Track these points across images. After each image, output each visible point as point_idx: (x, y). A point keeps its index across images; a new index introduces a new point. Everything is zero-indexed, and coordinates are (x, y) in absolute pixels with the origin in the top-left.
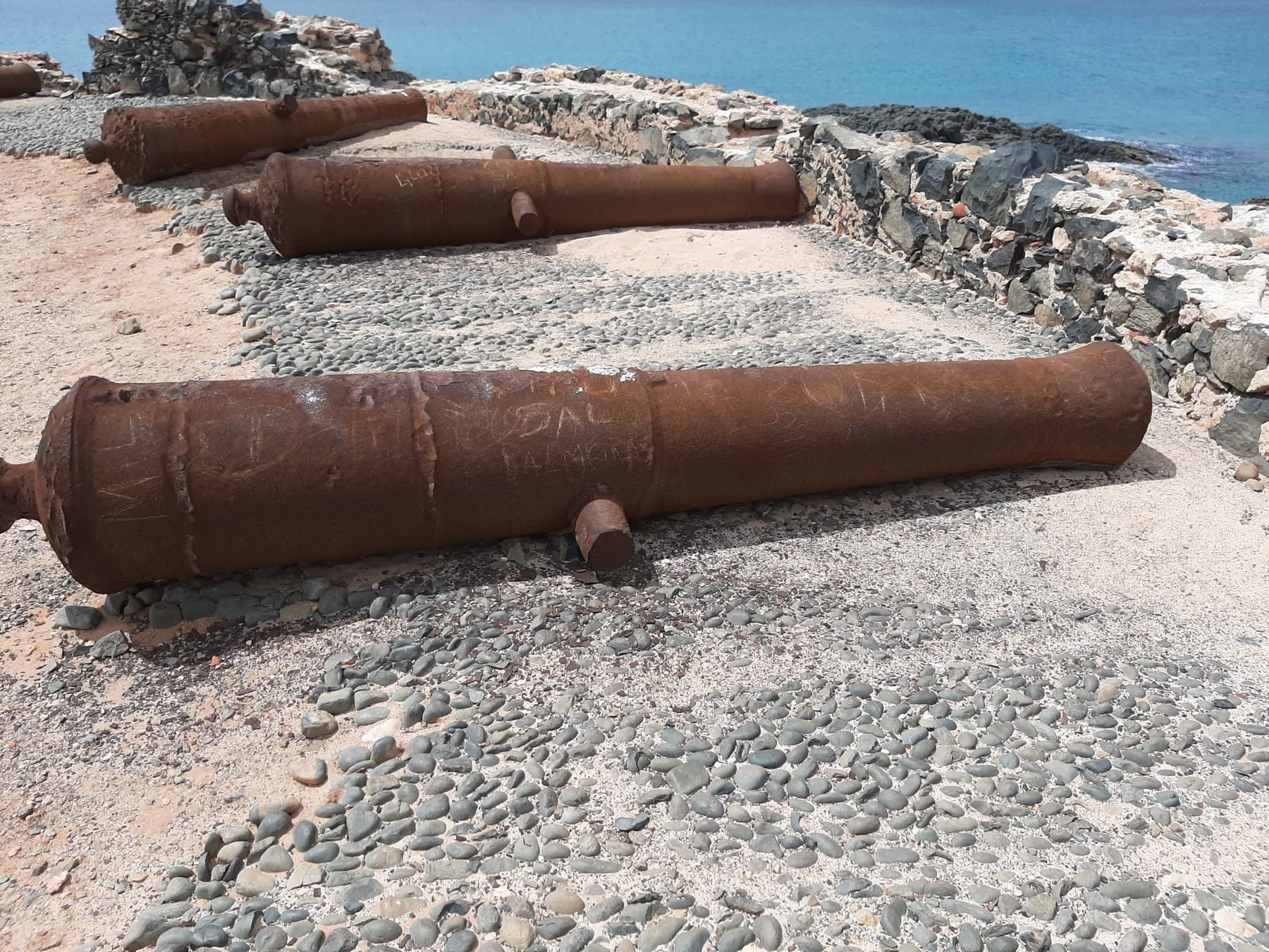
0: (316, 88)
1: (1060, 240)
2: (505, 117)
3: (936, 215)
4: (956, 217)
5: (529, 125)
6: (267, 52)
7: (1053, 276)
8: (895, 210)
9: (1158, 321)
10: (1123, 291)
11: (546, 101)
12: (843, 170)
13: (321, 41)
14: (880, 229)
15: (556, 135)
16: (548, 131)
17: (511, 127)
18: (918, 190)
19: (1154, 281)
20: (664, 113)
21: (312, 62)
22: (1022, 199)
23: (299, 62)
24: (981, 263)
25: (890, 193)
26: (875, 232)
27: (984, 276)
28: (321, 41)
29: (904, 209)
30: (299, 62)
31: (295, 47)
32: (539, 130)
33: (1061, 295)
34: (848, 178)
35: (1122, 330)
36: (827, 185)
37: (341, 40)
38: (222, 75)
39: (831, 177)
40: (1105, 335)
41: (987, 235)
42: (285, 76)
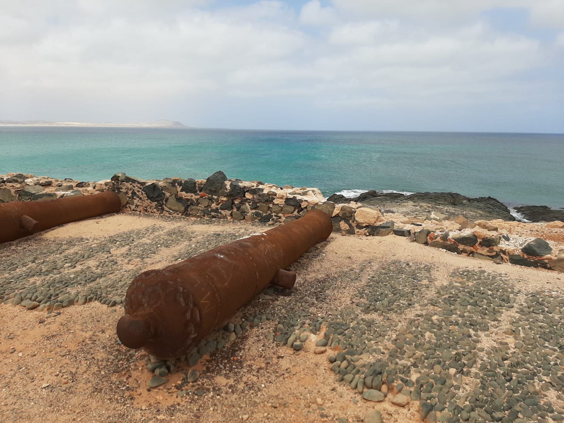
1: (248, 196)
3: (193, 198)
4: (201, 197)
7: (249, 207)
8: (172, 200)
9: (293, 209)
10: (277, 204)
12: (140, 190)
14: (165, 207)
18: (182, 191)
19: (287, 200)
20: (10, 182)
22: (228, 187)
24: (217, 209)
25: (168, 194)
26: (163, 209)
27: (220, 213)
29: (176, 198)
33: (254, 211)
34: (144, 192)
35: (280, 215)
36: (132, 196)
39: (134, 193)
40: (274, 217)
41: (217, 200)
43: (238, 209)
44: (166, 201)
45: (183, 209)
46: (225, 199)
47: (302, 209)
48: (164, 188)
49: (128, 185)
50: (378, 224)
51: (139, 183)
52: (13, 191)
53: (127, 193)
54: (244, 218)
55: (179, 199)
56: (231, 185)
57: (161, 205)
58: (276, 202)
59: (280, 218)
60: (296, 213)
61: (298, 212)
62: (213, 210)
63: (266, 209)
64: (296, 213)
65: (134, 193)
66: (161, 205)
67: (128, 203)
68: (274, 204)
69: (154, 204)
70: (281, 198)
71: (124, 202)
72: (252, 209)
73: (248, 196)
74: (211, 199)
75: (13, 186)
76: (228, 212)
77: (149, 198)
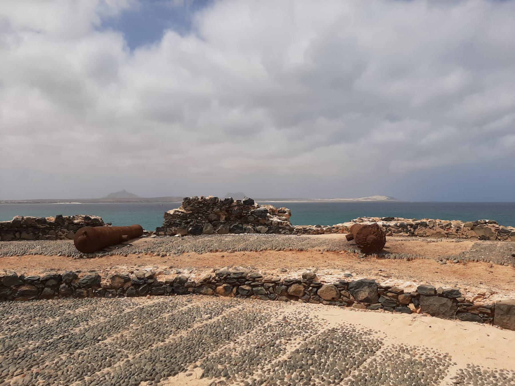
0: (280, 228)
5: (401, 234)
6: (256, 217)
11: (411, 226)
13: (273, 212)
15: (416, 236)
16: (413, 235)
20: (491, 223)
21: (275, 219)
23: (271, 219)
28: (273, 212)
30: (271, 219)
31: (268, 214)
32: (407, 235)
37: (279, 212)
38: (230, 226)
42: (264, 224)
52: (493, 229)
75: (493, 226)
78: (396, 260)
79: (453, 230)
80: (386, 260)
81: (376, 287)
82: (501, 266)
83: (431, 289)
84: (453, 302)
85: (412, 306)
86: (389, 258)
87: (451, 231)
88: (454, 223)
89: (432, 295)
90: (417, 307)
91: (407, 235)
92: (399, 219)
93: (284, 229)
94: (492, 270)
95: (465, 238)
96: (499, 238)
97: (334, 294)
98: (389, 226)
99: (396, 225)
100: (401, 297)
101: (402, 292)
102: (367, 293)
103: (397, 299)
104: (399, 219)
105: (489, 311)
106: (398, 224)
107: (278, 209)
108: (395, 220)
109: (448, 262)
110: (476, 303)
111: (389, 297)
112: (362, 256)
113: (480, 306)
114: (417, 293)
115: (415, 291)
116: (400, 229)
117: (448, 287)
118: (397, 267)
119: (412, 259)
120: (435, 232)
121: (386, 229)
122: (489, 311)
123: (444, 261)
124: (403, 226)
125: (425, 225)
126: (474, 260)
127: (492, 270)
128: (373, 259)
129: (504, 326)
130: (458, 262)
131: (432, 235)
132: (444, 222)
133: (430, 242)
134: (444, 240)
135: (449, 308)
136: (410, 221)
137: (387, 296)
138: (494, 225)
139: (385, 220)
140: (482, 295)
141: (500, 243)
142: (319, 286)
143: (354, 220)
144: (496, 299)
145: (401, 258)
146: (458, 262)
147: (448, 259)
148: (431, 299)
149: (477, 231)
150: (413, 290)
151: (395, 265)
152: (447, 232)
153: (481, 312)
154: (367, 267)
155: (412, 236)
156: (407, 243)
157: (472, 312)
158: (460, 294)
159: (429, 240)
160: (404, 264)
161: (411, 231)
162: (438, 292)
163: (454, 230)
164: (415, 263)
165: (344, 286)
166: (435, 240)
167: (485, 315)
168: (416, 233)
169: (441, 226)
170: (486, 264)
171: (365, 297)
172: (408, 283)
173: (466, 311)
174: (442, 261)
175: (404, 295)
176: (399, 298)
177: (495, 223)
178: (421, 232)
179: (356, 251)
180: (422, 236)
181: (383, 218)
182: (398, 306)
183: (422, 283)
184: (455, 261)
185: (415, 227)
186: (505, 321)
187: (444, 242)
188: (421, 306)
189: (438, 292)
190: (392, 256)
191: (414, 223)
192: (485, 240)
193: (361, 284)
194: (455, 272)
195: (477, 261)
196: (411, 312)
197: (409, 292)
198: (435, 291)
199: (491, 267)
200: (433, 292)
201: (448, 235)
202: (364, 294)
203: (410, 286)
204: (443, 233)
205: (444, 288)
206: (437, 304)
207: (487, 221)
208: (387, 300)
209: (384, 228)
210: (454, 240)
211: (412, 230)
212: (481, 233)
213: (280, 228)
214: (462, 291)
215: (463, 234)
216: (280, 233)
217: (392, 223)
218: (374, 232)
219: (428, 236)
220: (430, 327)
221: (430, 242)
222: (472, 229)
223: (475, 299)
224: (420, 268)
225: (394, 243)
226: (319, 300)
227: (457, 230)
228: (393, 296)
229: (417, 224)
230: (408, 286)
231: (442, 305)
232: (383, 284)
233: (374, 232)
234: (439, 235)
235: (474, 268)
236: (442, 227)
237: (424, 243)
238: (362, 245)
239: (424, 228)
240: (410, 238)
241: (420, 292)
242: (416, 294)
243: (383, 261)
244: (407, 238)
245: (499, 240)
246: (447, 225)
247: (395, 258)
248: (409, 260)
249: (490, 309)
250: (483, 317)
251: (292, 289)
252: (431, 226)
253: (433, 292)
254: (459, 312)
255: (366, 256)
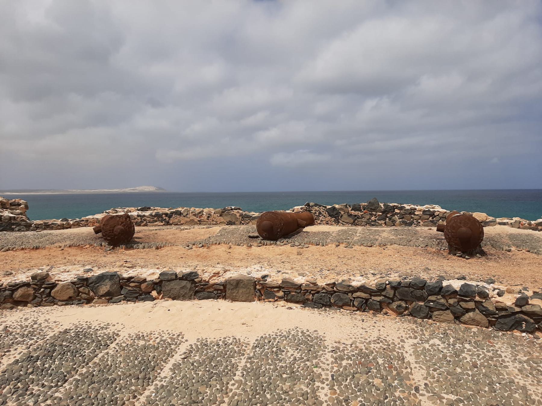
2: (142, 222)
5: (156, 223)
8: (345, 216)
10: (417, 215)
11: (166, 214)
15: (171, 224)
16: (168, 223)
17: (146, 225)
19: (424, 211)
20: (236, 209)
25: (342, 213)
26: (339, 222)
32: (162, 224)
33: (401, 220)
35: (419, 221)
37: (11, 204)
39: (320, 213)
40: (415, 223)
43: (390, 219)
44: (341, 217)
45: (352, 221)
46: (381, 214)
47: (435, 216)
48: (341, 209)
49: (316, 208)
50: (488, 220)
51: (324, 207)
53: (315, 213)
54: (394, 225)
55: (350, 215)
56: (384, 205)
57: (338, 220)
58: (416, 213)
59: (419, 223)
60: (431, 219)
61: (433, 218)
62: (372, 221)
63: (410, 218)
64: (431, 219)
65: (320, 213)
66: (338, 220)
67: (316, 219)
68: (415, 215)
69: (333, 219)
70: (420, 211)
71: (315, 217)
72: (399, 219)
73: (397, 211)
74: (372, 215)
76: (383, 222)
77: (330, 215)
78: (144, 250)
79: (205, 217)
80: (135, 251)
81: (118, 279)
82: (238, 247)
83: (172, 274)
84: (192, 284)
85: (154, 293)
86: (138, 249)
87: (202, 218)
88: (206, 210)
89: (173, 280)
90: (159, 293)
91: (162, 224)
92: (156, 208)
93: (18, 225)
94: (230, 251)
95: (215, 224)
96: (243, 222)
97: (71, 293)
98: (144, 216)
99: (151, 215)
100: (143, 286)
101: (145, 281)
102: (108, 287)
103: (140, 288)
104: (156, 208)
105: (222, 288)
106: (154, 214)
107: (10, 202)
108: (152, 210)
109: (194, 247)
110: (212, 282)
111: (132, 287)
112: (109, 249)
113: (215, 284)
114: (159, 280)
115: (157, 277)
116: (155, 219)
117: (187, 270)
118: (145, 257)
119: (161, 247)
120: (188, 220)
121: (141, 219)
122: (222, 288)
123: (191, 246)
124: (158, 215)
125: (180, 214)
126: (216, 244)
127: (230, 251)
128: (121, 250)
129: (234, 300)
130: (203, 246)
131: (186, 223)
132: (198, 210)
133: (183, 229)
134: (196, 227)
135: (188, 290)
136: (166, 210)
137: (129, 286)
138: (239, 211)
139: (142, 210)
140: (217, 274)
141: (242, 227)
142: (54, 285)
143: (107, 211)
144: (228, 276)
145: (150, 247)
146: (203, 246)
147: (194, 244)
148: (173, 284)
149: (225, 217)
150: (155, 277)
151: (143, 254)
152: (199, 219)
153: (215, 290)
154: (113, 260)
155: (167, 225)
156: (162, 233)
157: (209, 290)
158: (198, 275)
159: (182, 228)
160: (153, 252)
161: (165, 220)
162: (179, 276)
163: (206, 218)
164: (163, 252)
165: (83, 282)
166: (188, 227)
167: (219, 292)
168: (171, 222)
169: (194, 213)
170: (226, 245)
171: (106, 291)
172: (151, 271)
173: (203, 290)
174: (188, 246)
175: (146, 283)
176: (142, 287)
177: (240, 209)
178: (176, 220)
179: (103, 244)
180: (177, 225)
181: (139, 208)
182: (141, 295)
183: (164, 270)
184: (201, 245)
185: (170, 216)
186: (234, 294)
187: (197, 229)
188: (163, 292)
189: (179, 276)
190: (141, 246)
191: (169, 212)
192: (232, 224)
193: (101, 278)
194: (198, 256)
195: (219, 244)
196: (153, 299)
197: (152, 279)
198: (176, 275)
199: (230, 248)
200: (174, 277)
201: (200, 222)
202: (104, 288)
203: (153, 273)
204: (196, 220)
205: (184, 271)
206: (178, 287)
207: (233, 207)
208: (130, 290)
209: (139, 218)
210: (205, 227)
211: (167, 219)
212: (228, 219)
213: (13, 224)
214: (200, 272)
215: (213, 221)
216: (13, 230)
217: (147, 213)
218: (122, 223)
219: (182, 224)
220: (169, 310)
221: (183, 229)
222: (221, 216)
223: (210, 278)
224: (166, 255)
225: (148, 233)
226: (53, 302)
227: (208, 217)
228: (135, 286)
229: (172, 213)
230: (151, 274)
231: (182, 288)
232: (125, 275)
233: (122, 223)
234: (192, 223)
235: (215, 251)
236: (195, 215)
237: (178, 231)
238: (109, 237)
239: (178, 216)
240: (164, 227)
241: (162, 278)
242: (158, 281)
243: (131, 252)
244: (161, 227)
245: (243, 224)
246: (200, 213)
247: (144, 248)
248: (157, 248)
249: (223, 285)
250: (217, 293)
251: (18, 294)
252: (185, 214)
253: (174, 277)
254: (196, 292)
255: (113, 248)
